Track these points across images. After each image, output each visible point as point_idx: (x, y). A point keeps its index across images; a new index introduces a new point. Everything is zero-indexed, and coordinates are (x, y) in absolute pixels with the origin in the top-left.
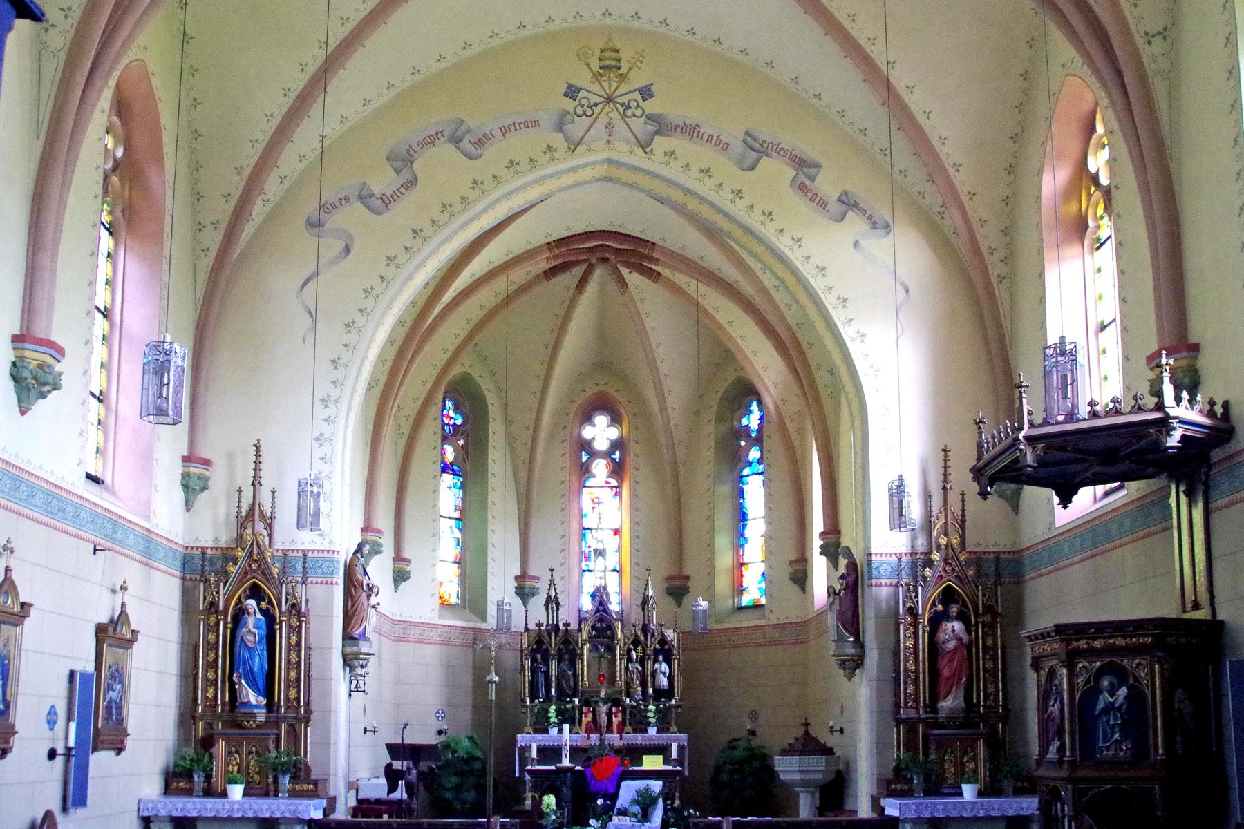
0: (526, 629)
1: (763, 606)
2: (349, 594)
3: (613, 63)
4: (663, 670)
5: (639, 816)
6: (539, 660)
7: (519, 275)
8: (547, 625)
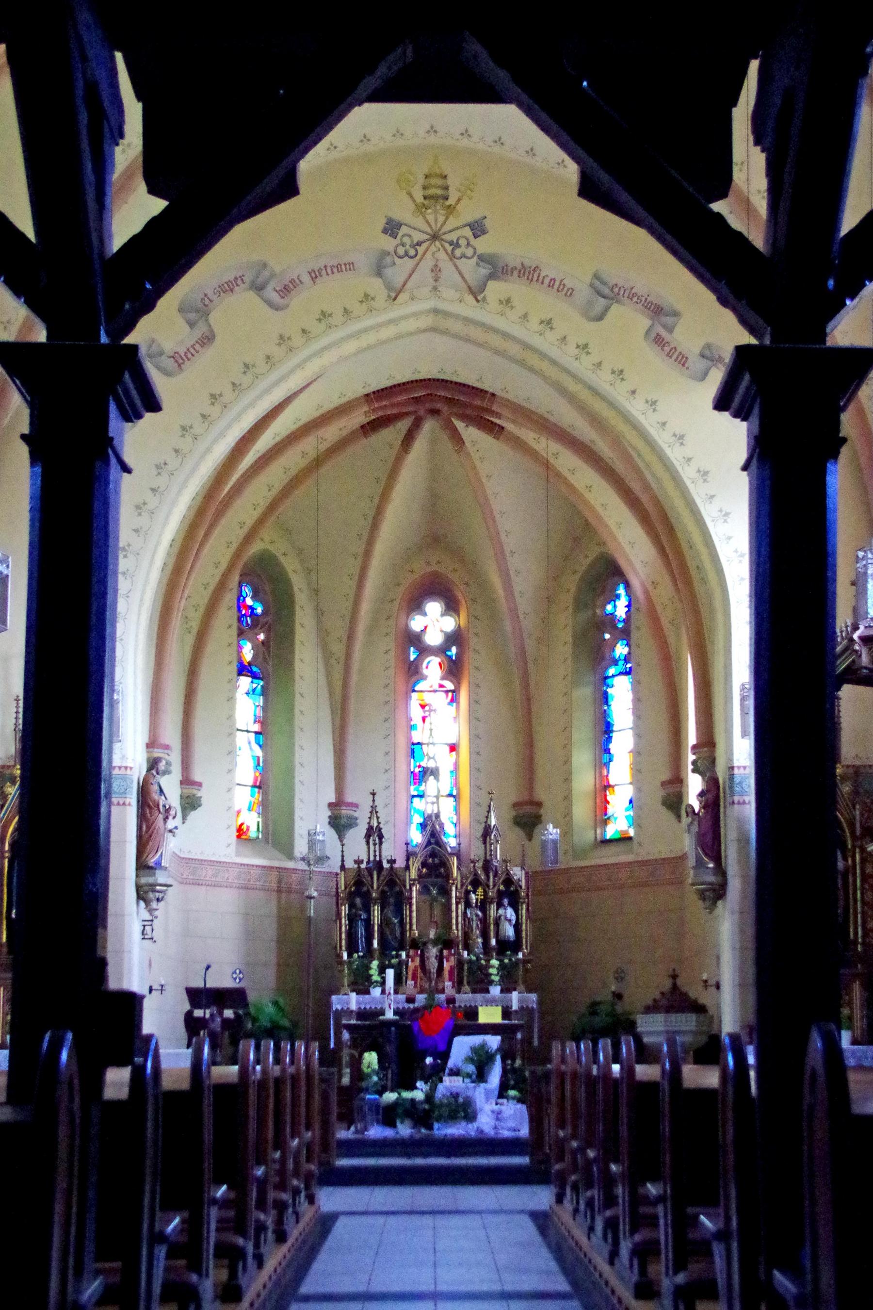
0: (343, 867)
1: (630, 838)
2: (142, 817)
3: (439, 192)
4: (508, 916)
5: (474, 1076)
7: (332, 433)
8: (368, 862)
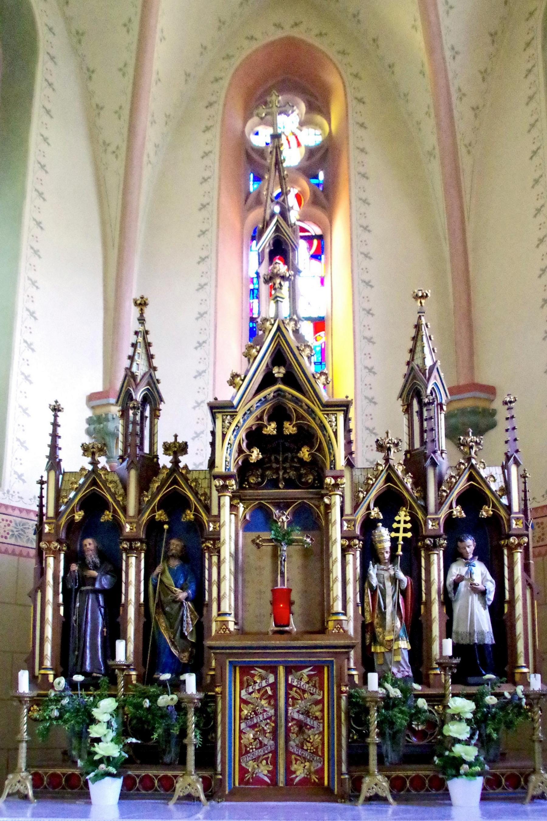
4: (477, 580)
6: (91, 556)
